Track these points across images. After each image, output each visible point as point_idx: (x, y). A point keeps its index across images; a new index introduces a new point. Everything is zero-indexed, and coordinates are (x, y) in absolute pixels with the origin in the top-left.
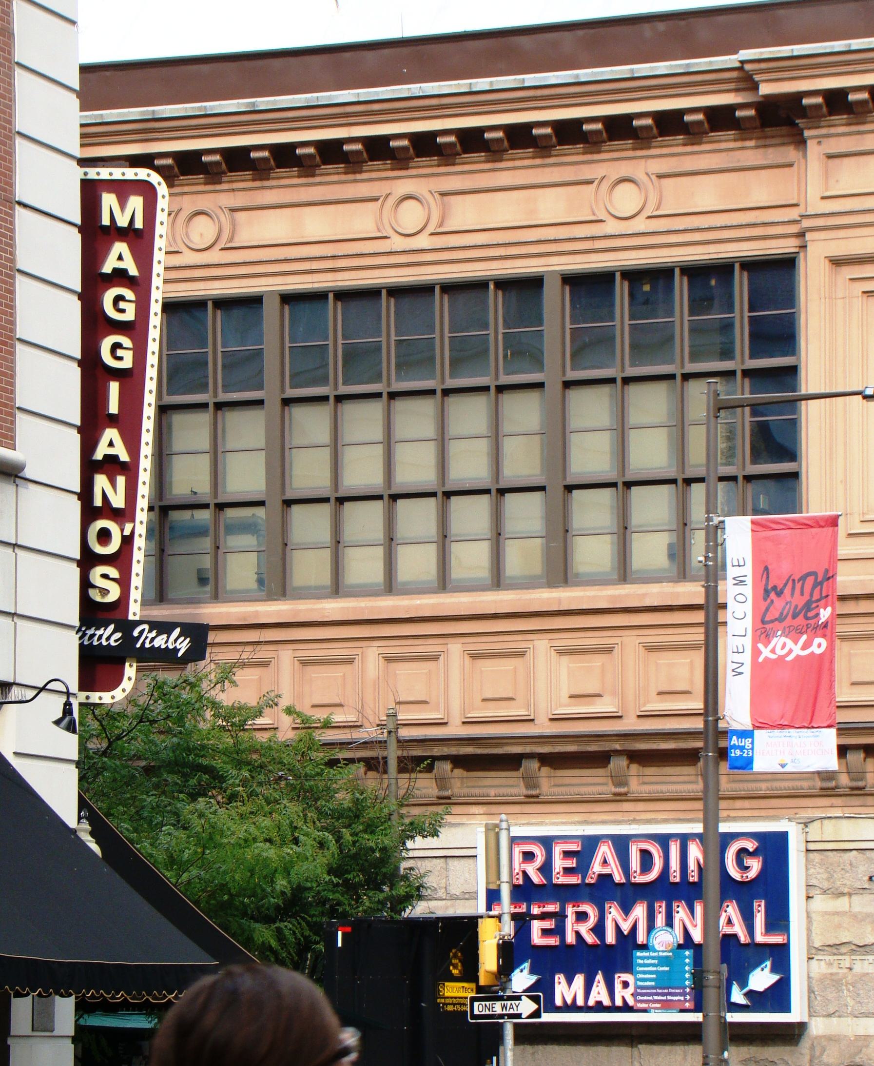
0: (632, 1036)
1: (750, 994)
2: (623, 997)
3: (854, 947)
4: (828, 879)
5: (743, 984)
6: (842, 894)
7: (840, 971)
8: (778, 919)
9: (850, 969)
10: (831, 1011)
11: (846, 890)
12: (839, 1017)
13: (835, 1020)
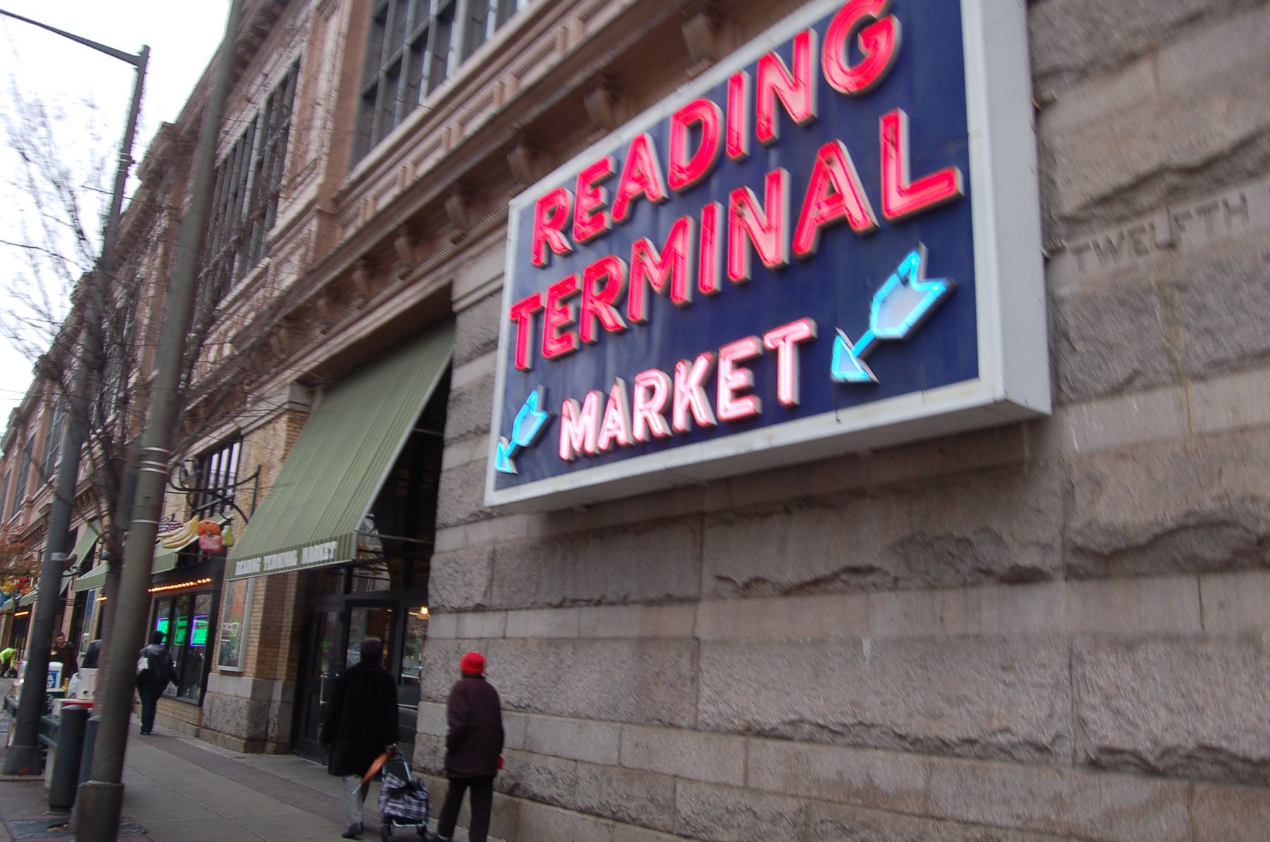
0: (703, 514)
1: (879, 353)
2: (646, 420)
3: (1172, 179)
4: (1089, 37)
5: (857, 326)
6: (1131, 58)
7: (1141, 261)
8: (943, 141)
9: (1171, 245)
10: (1118, 372)
11: (1141, 43)
12: (1148, 388)
13: (1133, 403)
